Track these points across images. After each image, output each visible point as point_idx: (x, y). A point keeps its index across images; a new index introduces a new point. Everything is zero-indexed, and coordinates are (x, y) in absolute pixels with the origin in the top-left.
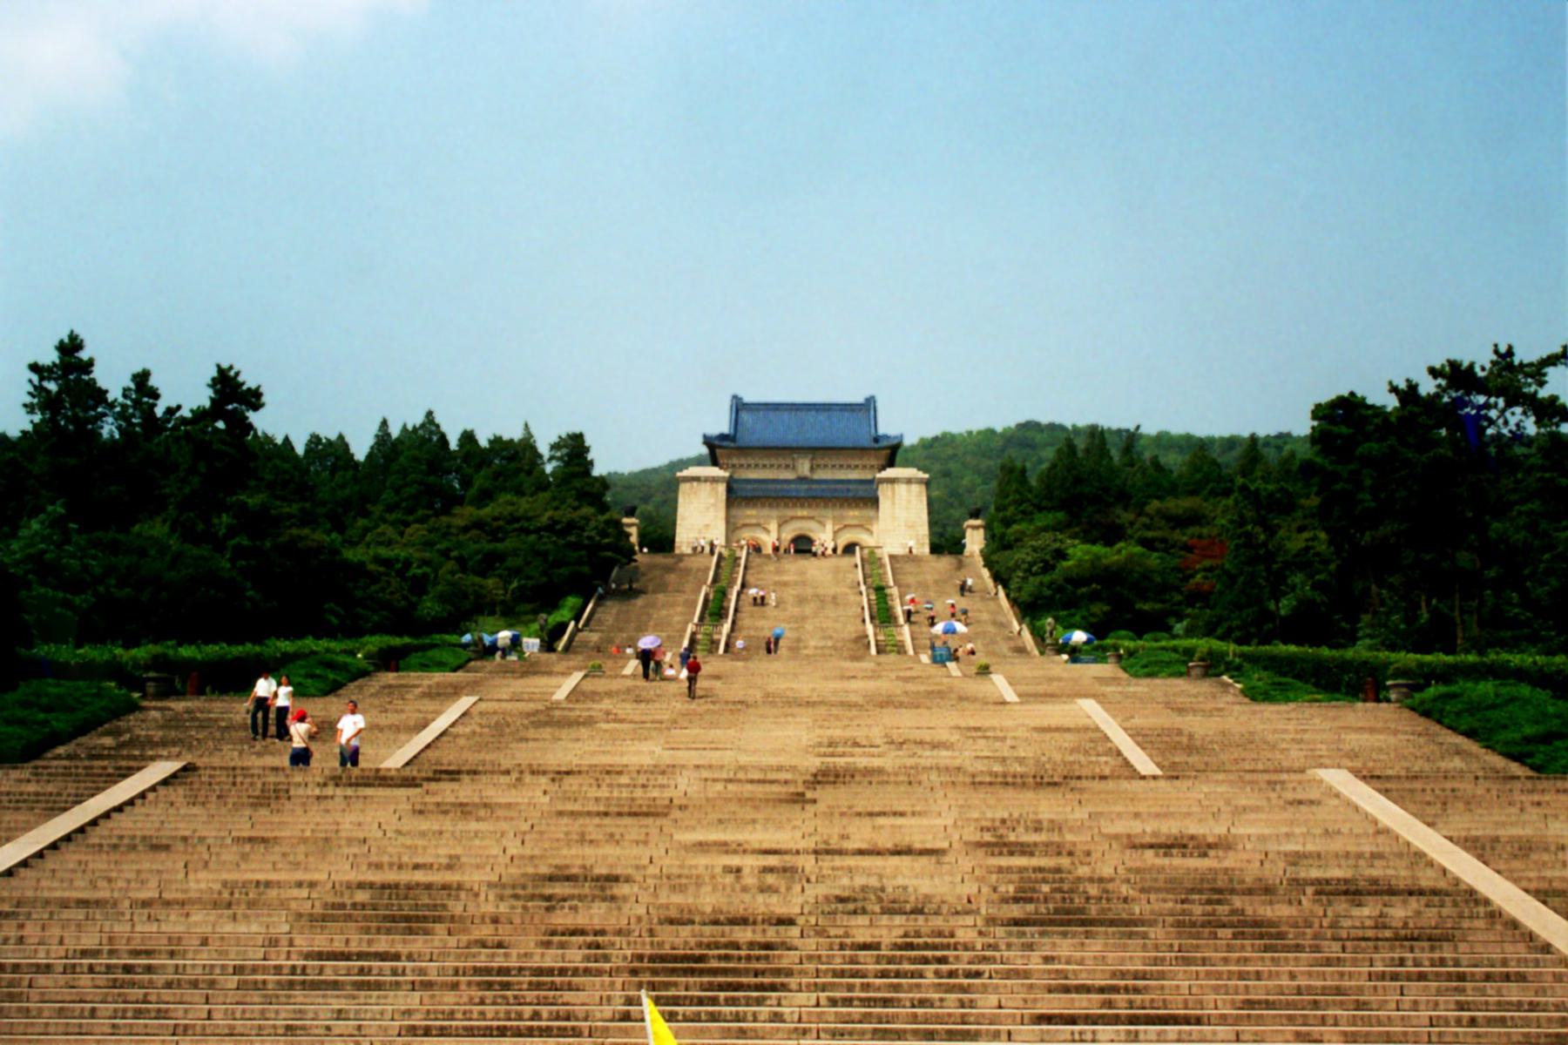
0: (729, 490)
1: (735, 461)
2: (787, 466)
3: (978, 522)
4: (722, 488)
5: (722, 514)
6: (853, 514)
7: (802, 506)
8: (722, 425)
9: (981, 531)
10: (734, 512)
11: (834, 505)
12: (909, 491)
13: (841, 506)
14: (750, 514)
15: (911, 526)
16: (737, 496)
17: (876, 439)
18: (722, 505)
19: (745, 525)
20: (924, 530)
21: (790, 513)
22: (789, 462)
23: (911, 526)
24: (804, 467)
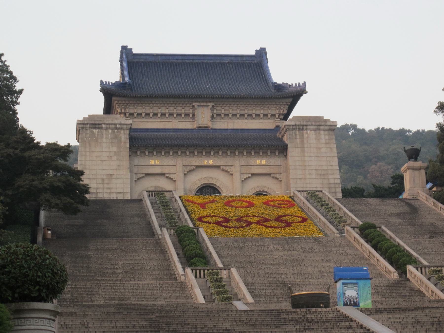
0: (132, 139)
1: (131, 110)
2: (187, 115)
3: (418, 164)
4: (124, 136)
5: (126, 162)
6: (260, 163)
7: (208, 154)
8: (114, 75)
9: (423, 172)
10: (138, 160)
11: (241, 153)
12: (318, 139)
13: (249, 154)
14: (154, 163)
15: (323, 175)
16: (141, 143)
17: (279, 87)
18: (126, 152)
19: (147, 175)
20: (336, 178)
21: (196, 161)
22: (189, 111)
23: (323, 175)
24: (203, 116)
